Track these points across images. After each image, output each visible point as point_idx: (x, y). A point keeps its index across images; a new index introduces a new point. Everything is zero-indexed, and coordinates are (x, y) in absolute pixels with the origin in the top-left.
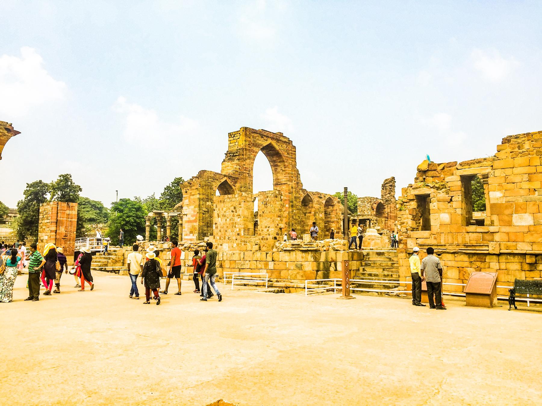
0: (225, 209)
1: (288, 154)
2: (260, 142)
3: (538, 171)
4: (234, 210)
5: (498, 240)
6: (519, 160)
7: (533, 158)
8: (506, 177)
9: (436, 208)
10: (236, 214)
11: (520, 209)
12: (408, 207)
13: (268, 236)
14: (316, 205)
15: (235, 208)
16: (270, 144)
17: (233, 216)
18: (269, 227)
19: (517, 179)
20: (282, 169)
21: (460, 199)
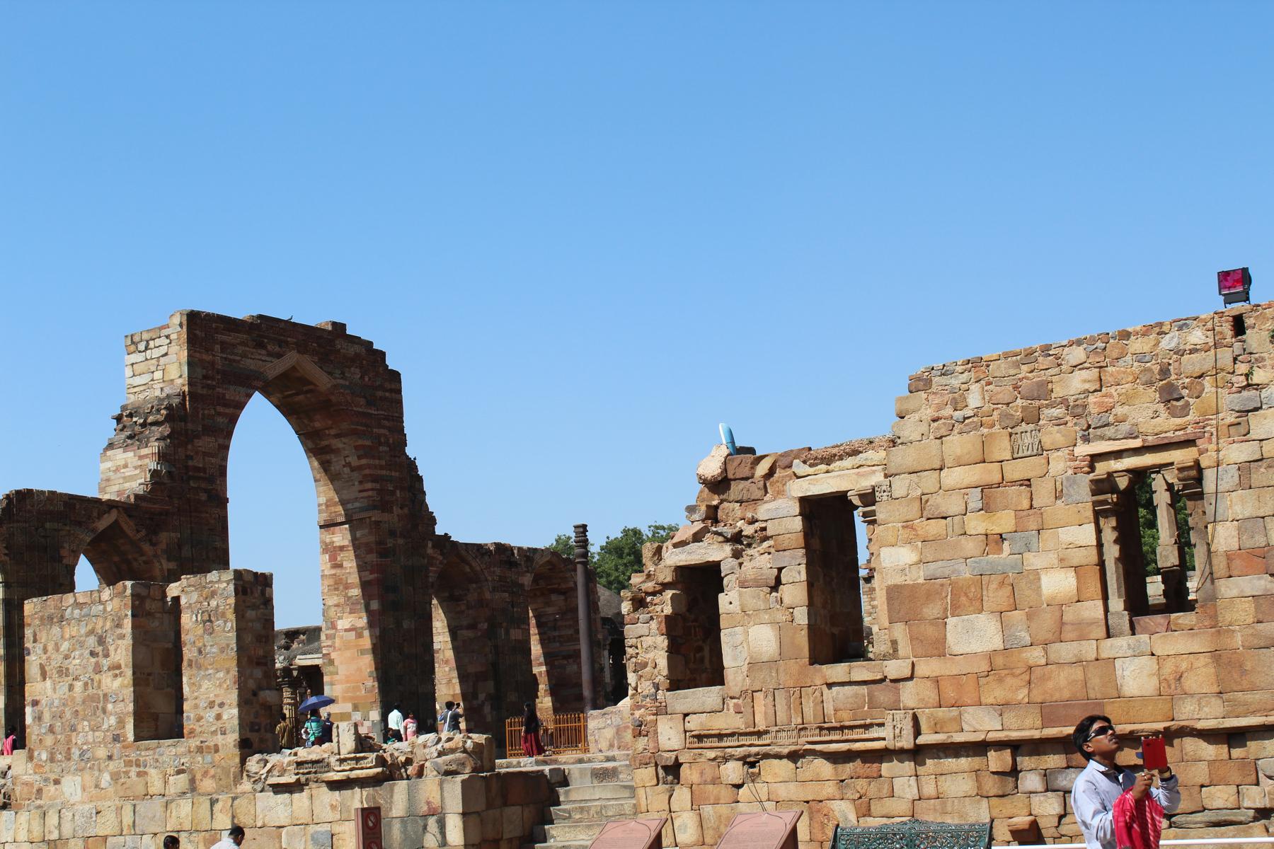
0: (65, 646)
1: (370, 403)
2: (250, 364)
3: (1008, 477)
4: (99, 649)
5: (911, 704)
6: (958, 444)
7: (991, 435)
8: (922, 501)
9: (736, 607)
10: (105, 663)
11: (964, 598)
12: (658, 608)
13: (219, 739)
14: (497, 596)
15: (101, 641)
16: (294, 368)
17: (98, 670)
18: (222, 705)
19: (953, 505)
20: (348, 465)
21: (804, 576)
